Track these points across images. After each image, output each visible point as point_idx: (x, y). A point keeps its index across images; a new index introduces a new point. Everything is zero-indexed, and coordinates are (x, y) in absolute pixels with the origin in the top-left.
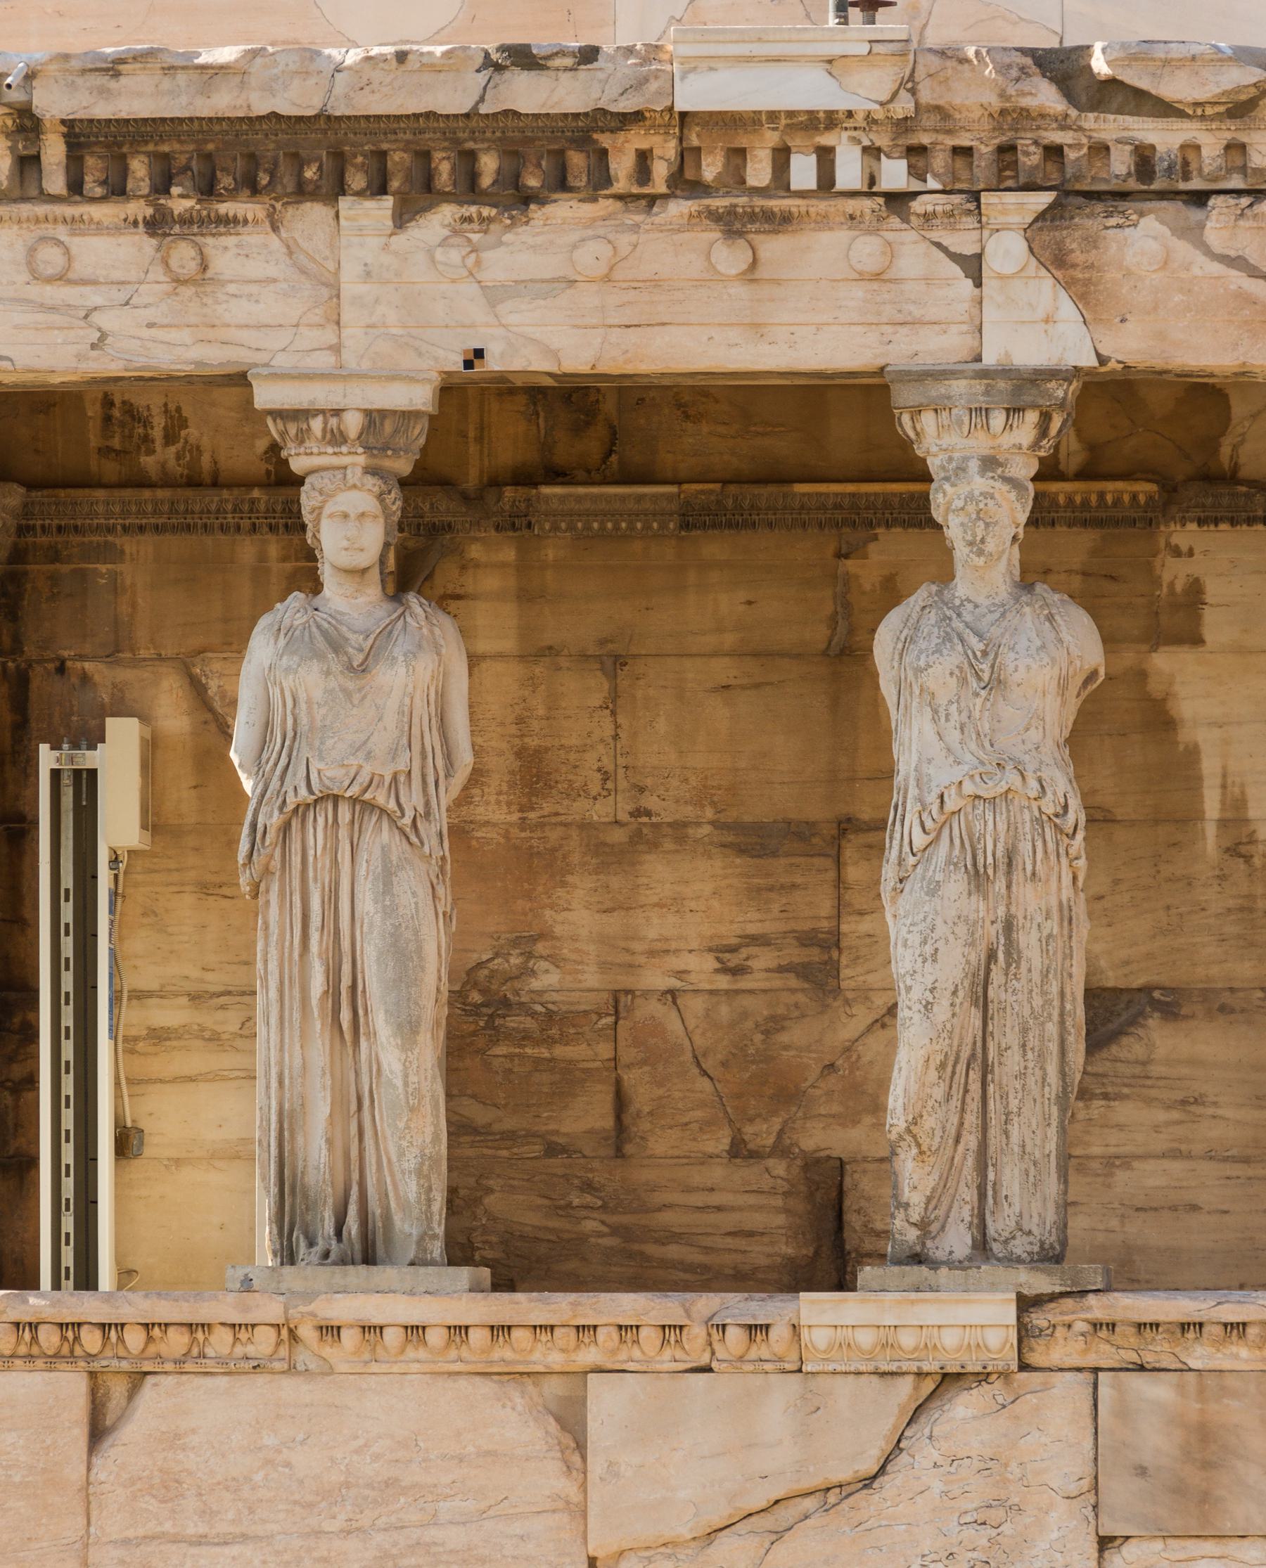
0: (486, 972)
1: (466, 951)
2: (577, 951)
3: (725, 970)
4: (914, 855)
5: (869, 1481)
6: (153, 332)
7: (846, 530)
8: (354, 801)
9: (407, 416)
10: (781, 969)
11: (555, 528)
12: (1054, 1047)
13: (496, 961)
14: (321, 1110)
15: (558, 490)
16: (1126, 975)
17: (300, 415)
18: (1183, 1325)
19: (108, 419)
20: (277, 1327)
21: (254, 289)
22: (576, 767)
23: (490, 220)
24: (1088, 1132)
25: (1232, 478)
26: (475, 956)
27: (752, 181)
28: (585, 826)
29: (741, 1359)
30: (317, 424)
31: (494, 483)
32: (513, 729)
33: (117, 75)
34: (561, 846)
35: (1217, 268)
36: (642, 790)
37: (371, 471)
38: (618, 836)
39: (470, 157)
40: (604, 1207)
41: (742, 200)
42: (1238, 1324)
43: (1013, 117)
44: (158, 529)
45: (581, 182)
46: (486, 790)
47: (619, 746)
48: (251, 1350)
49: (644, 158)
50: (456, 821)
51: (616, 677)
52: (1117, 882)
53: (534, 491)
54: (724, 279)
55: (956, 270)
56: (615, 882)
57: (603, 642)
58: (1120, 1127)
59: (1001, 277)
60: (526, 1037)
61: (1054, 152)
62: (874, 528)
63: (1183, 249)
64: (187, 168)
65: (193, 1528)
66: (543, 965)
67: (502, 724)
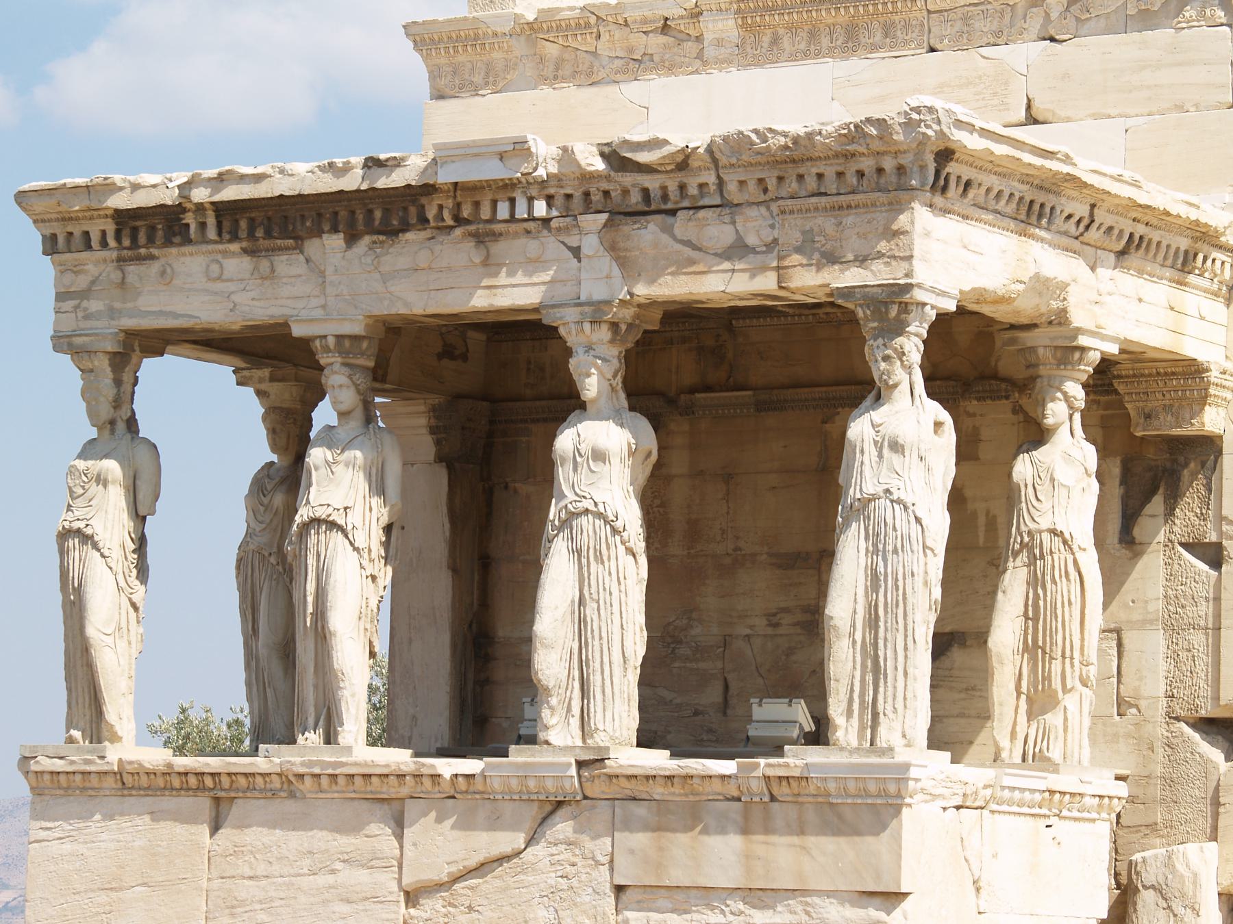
3: (771, 625)
5: (518, 853)
6: (255, 303)
8: (326, 522)
9: (355, 338)
10: (795, 625)
14: (311, 670)
19: (528, 369)
21: (293, 280)
25: (995, 376)
27: (483, 217)
30: (317, 343)
33: (222, 180)
35: (679, 247)
36: (737, 538)
37: (345, 364)
38: (728, 561)
39: (370, 212)
40: (717, 741)
41: (481, 226)
43: (588, 177)
44: (545, 420)
45: (413, 220)
48: (272, 786)
49: (441, 207)
54: (475, 265)
59: (588, 257)
61: (606, 193)
63: (665, 238)
64: (262, 223)
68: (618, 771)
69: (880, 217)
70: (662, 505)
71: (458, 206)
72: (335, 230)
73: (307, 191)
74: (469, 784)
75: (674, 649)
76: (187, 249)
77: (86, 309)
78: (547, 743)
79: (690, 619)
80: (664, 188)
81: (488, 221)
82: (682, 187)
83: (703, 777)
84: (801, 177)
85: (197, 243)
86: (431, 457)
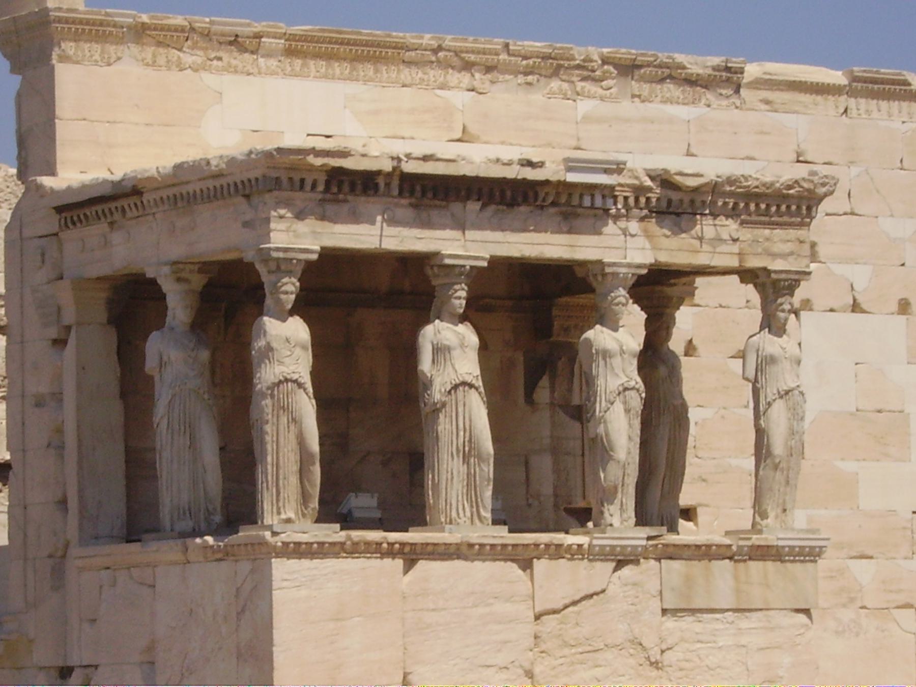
5: (603, 591)
17: (454, 266)
20: (457, 544)
23: (503, 211)
30: (457, 270)
41: (570, 208)
45: (532, 200)
49: (547, 194)
55: (620, 232)
59: (633, 236)
65: (432, 606)
69: (792, 233)
71: (558, 194)
72: (479, 200)
73: (482, 175)
76: (372, 199)
77: (294, 231)
78: (611, 525)
80: (681, 201)
81: (564, 205)
82: (692, 202)
84: (757, 205)
85: (384, 195)
86: (105, 321)
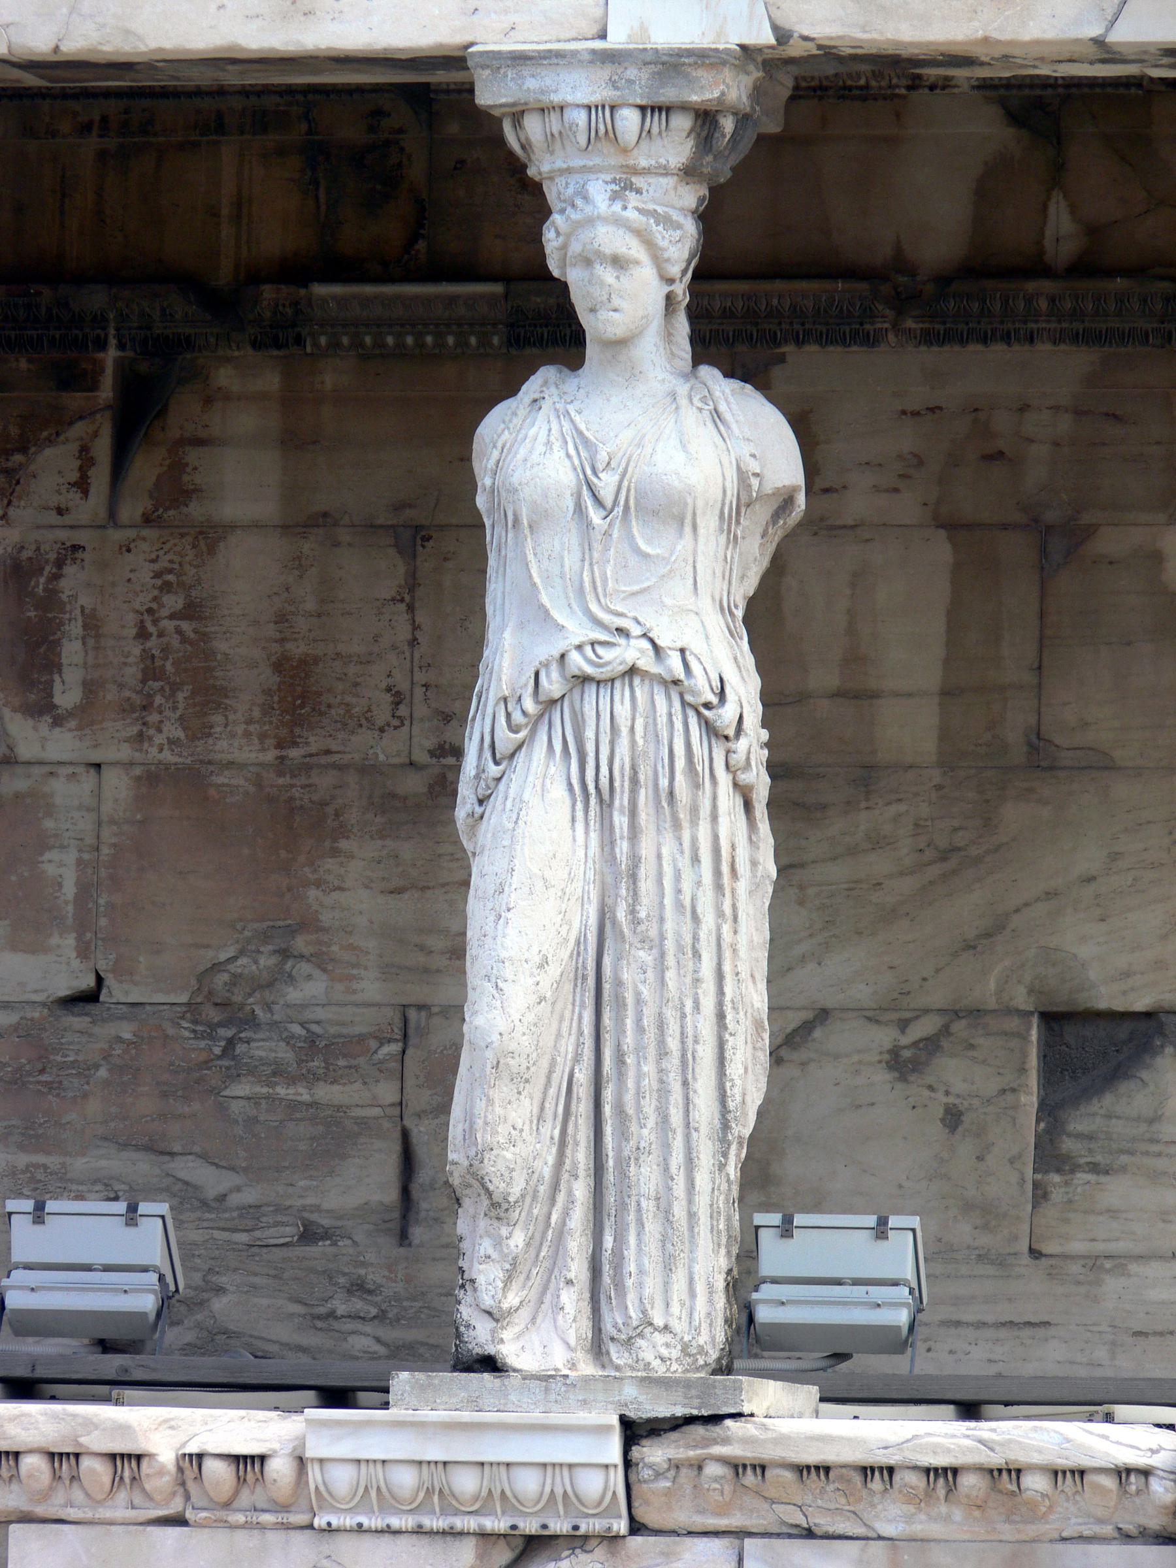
0: (225, 977)
1: (197, 946)
2: (351, 947)
4: (497, 763)
7: (741, 348)
11: (335, 345)
12: (706, 1053)
13: (239, 962)
15: (337, 289)
16: (1124, 993)
18: (864, 1469)
22: (356, 684)
24: (1067, 1221)
26: (211, 953)
28: (367, 769)
29: (227, 1505)
31: (254, 277)
32: (270, 630)
34: (333, 798)
40: (381, 1317)
42: (945, 1470)
46: (231, 717)
47: (417, 655)
50: (188, 761)
51: (414, 557)
52: (1115, 856)
53: (303, 292)
56: (407, 850)
57: (399, 507)
58: (1113, 1213)
60: (279, 1072)
62: (779, 345)
66: (305, 968)
67: (256, 623)
68: (767, 1453)
70: (191, 611)
74: (241, 1481)
75: (231, 1043)
79: (285, 954)
83: (1056, 1473)
